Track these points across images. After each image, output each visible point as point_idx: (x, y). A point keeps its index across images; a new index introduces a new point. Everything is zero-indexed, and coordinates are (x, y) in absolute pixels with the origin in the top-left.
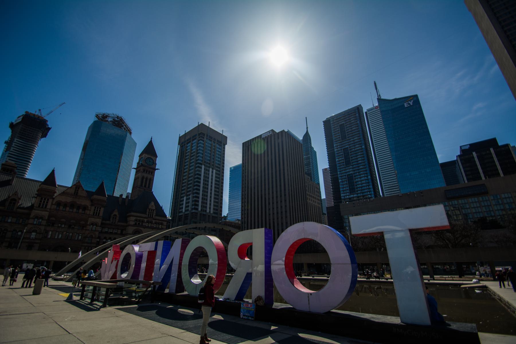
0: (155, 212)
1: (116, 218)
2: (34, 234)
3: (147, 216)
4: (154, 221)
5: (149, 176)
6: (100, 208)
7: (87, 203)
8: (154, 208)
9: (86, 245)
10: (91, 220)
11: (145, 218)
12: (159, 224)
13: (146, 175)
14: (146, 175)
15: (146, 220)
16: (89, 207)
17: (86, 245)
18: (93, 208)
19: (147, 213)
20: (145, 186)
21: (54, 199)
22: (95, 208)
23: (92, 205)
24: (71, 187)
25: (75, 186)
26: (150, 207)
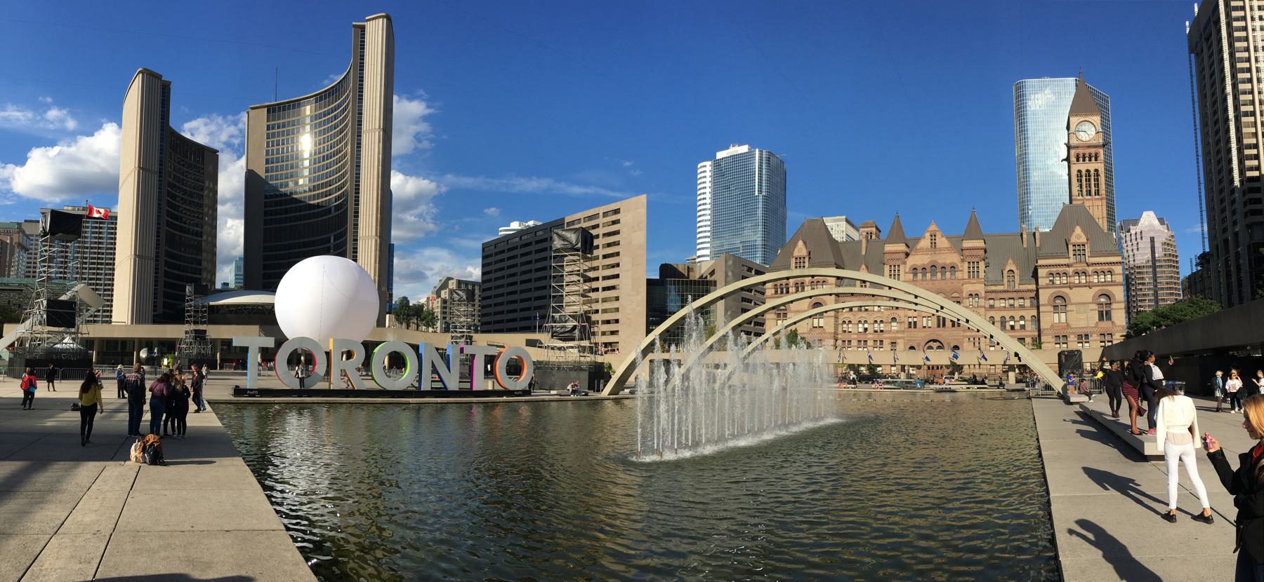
0: (1087, 248)
3: (1072, 260)
4: (1090, 269)
5: (1092, 166)
8: (1083, 240)
10: (968, 288)
11: (1068, 266)
13: (1083, 167)
14: (1083, 167)
15: (1070, 270)
18: (966, 265)
19: (1071, 253)
20: (1089, 193)
21: (905, 263)
23: (963, 261)
26: (1074, 240)
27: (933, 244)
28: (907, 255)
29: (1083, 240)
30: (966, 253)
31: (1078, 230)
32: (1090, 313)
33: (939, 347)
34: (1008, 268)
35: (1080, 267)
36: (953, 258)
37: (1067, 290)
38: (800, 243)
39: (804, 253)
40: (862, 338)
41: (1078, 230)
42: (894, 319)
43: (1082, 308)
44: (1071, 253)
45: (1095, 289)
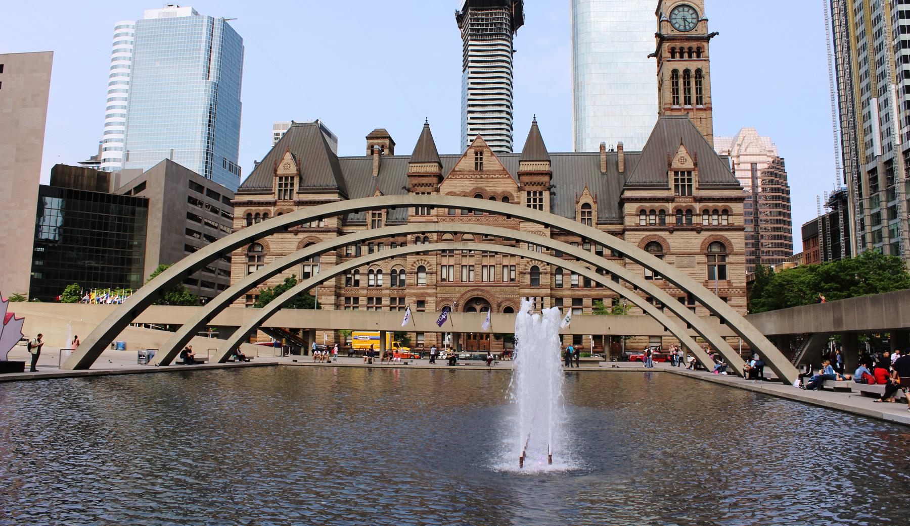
0: (694, 177)
1: (590, 213)
2: (422, 275)
3: (671, 193)
4: (698, 207)
6: (541, 194)
7: (508, 186)
8: (689, 165)
9: (527, 291)
12: (716, 212)
15: (670, 207)
16: (515, 195)
17: (527, 291)
18: (524, 195)
21: (438, 190)
22: (529, 193)
23: (520, 189)
24: (465, 155)
25: (473, 150)
26: (676, 164)
27: (479, 165)
28: (441, 179)
29: (689, 165)
30: (526, 179)
31: (682, 151)
32: (697, 268)
33: (485, 309)
34: (582, 201)
35: (684, 202)
36: (508, 186)
37: (665, 234)
38: (288, 156)
39: (293, 170)
40: (374, 293)
41: (682, 151)
42: (421, 269)
43: (686, 260)
44: (672, 184)
45: (705, 235)
